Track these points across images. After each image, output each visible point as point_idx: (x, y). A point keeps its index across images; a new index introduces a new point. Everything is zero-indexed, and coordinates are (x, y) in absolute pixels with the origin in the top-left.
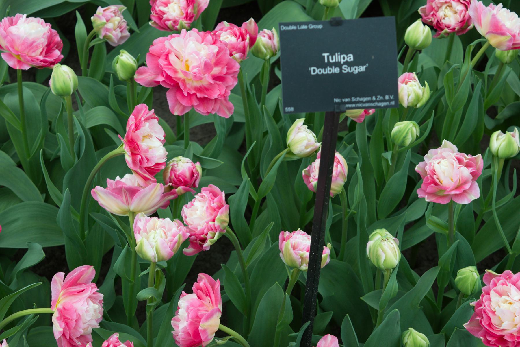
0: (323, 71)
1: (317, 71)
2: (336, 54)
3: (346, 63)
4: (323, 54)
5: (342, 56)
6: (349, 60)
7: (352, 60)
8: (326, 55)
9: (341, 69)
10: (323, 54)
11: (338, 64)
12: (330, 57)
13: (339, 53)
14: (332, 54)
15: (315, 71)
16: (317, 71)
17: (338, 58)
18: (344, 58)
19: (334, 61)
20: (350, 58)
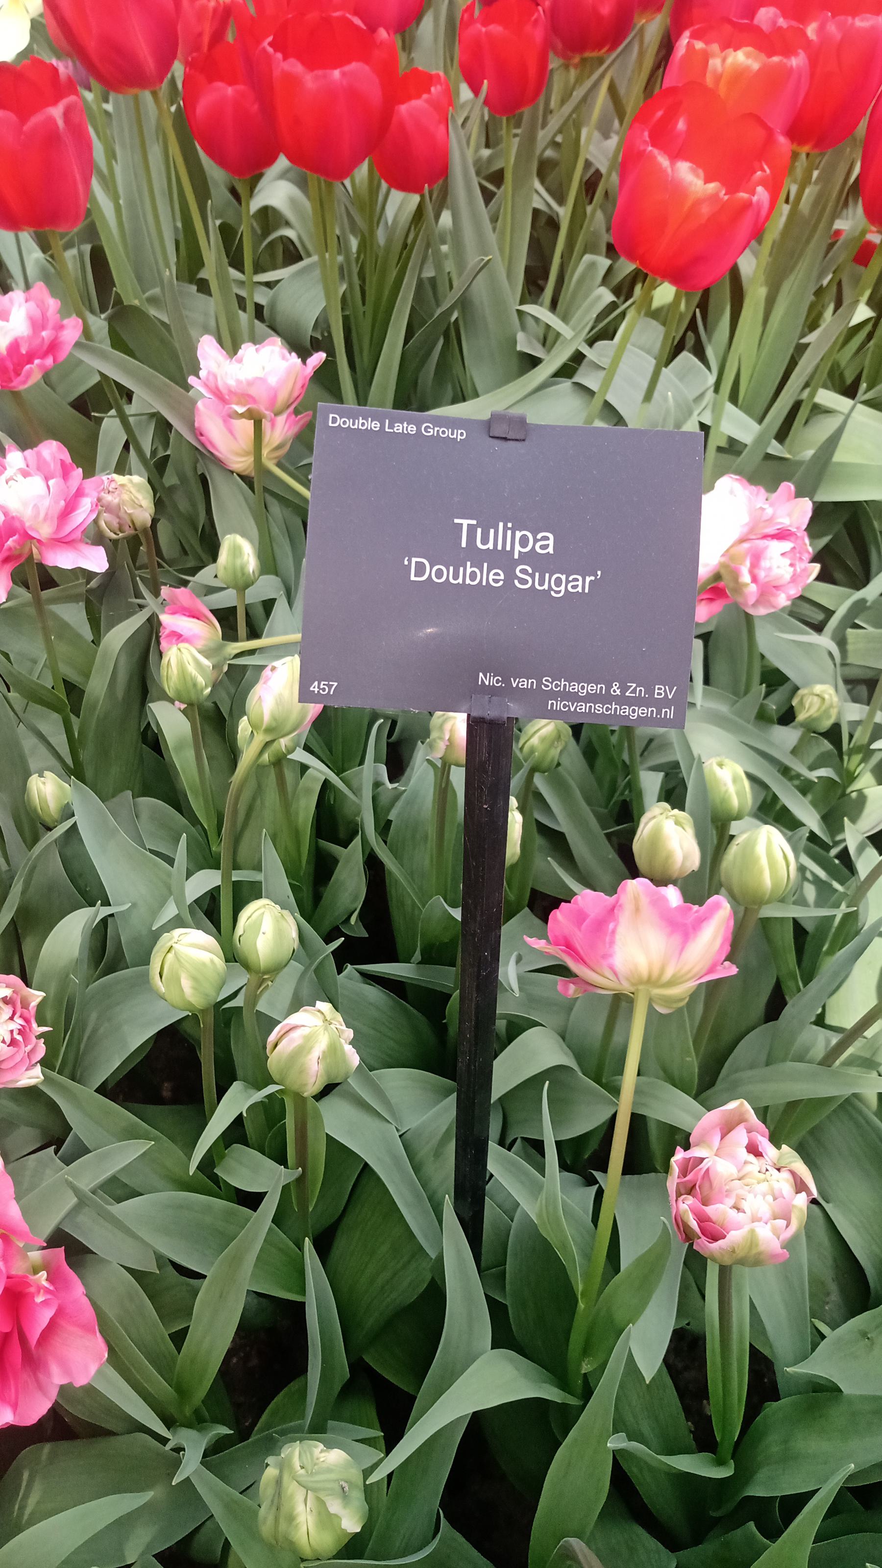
0: (448, 574)
1: (430, 572)
2: (501, 525)
3: (530, 558)
4: (456, 521)
7: (551, 550)
8: (465, 523)
9: (510, 576)
10: (456, 521)
11: (501, 559)
12: (479, 530)
13: (510, 525)
15: (423, 570)
16: (430, 572)
17: (503, 537)
18: (524, 542)
19: (490, 546)
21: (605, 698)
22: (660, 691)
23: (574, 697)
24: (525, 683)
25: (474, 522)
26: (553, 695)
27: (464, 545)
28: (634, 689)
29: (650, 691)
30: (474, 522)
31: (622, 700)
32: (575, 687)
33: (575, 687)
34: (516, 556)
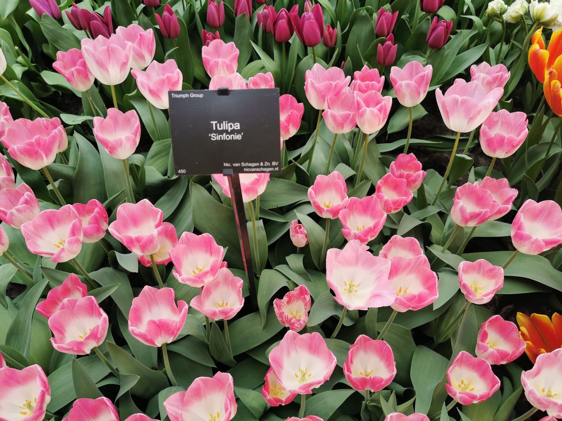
2: (224, 122)
4: (212, 122)
5: (229, 124)
6: (236, 129)
7: (239, 128)
8: (214, 123)
10: (212, 122)
11: (226, 131)
12: (218, 125)
14: (220, 122)
17: (226, 126)
18: (231, 126)
19: (222, 128)
20: (237, 126)
21: (259, 167)
22: (274, 163)
23: (251, 167)
24: (237, 165)
25: (216, 122)
26: (245, 167)
27: (214, 129)
28: (267, 164)
29: (271, 164)
30: (216, 122)
31: (264, 167)
32: (250, 165)
33: (250, 165)
34: (229, 131)
